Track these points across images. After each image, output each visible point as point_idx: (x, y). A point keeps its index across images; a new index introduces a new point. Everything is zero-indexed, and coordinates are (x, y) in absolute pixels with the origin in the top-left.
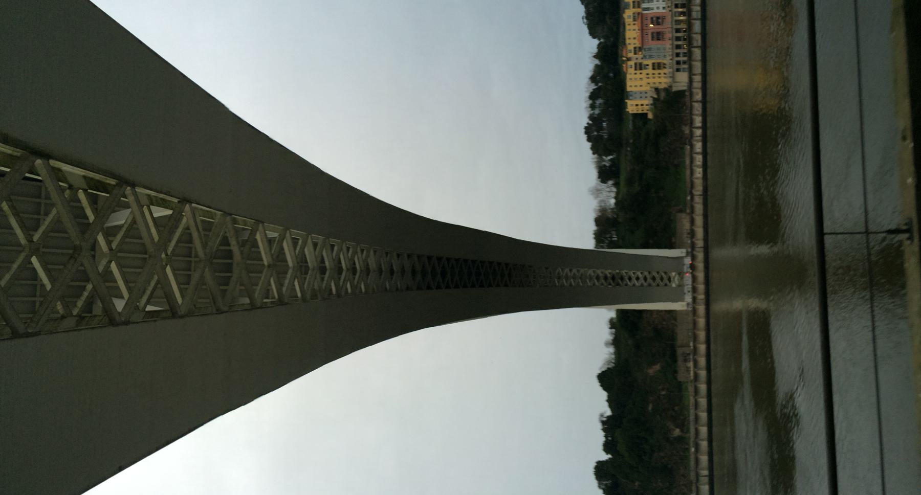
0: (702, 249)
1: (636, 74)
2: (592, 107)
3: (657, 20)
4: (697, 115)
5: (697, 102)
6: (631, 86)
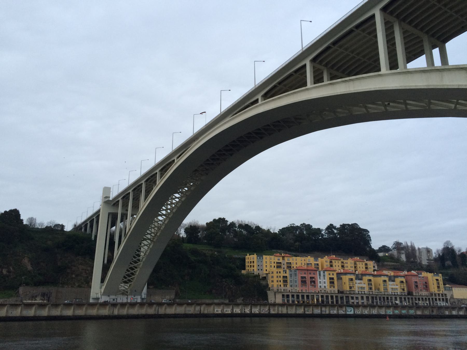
0: (157, 313)
1: (274, 263)
2: (241, 226)
3: (313, 282)
4: (260, 309)
5: (269, 309)
6: (266, 258)
